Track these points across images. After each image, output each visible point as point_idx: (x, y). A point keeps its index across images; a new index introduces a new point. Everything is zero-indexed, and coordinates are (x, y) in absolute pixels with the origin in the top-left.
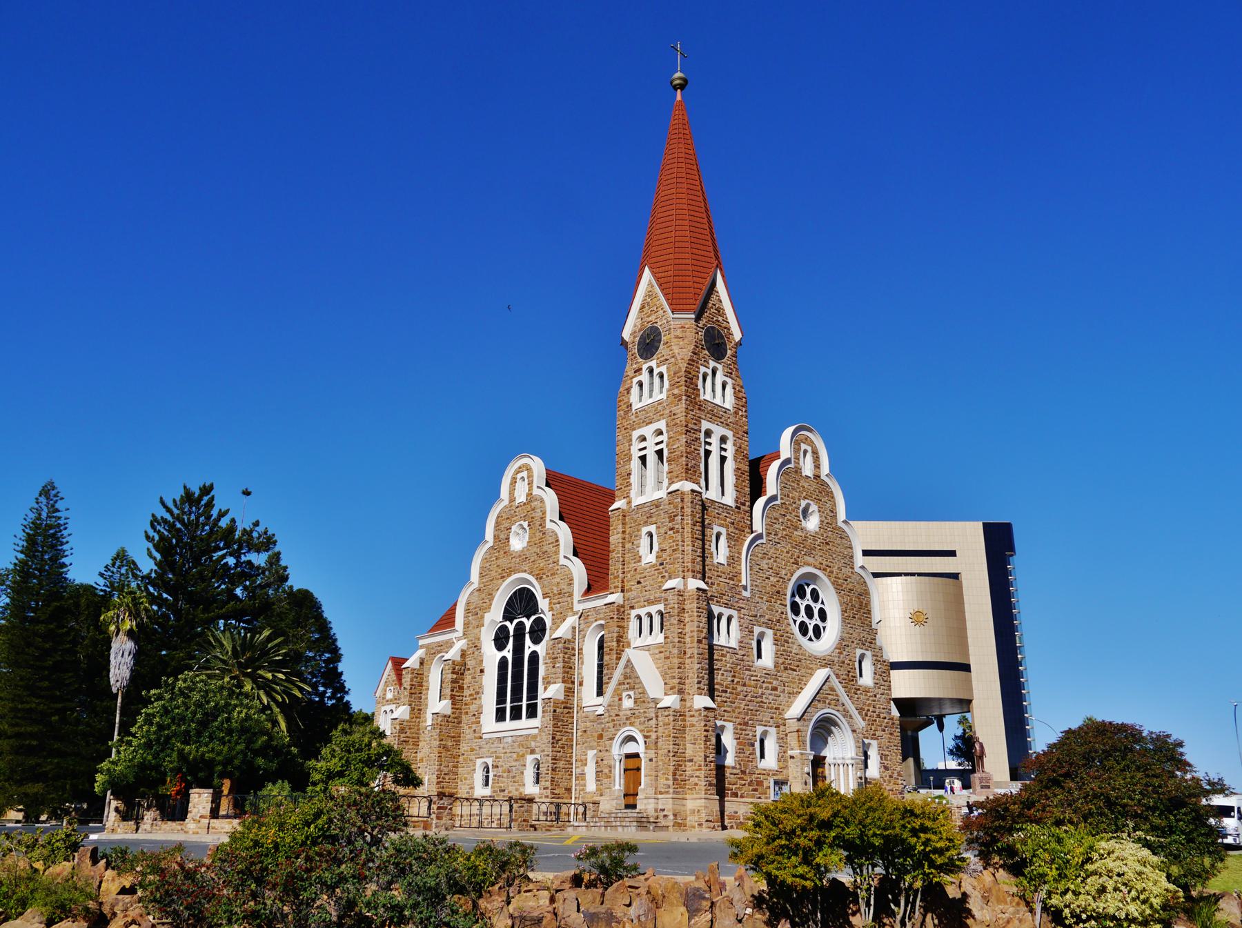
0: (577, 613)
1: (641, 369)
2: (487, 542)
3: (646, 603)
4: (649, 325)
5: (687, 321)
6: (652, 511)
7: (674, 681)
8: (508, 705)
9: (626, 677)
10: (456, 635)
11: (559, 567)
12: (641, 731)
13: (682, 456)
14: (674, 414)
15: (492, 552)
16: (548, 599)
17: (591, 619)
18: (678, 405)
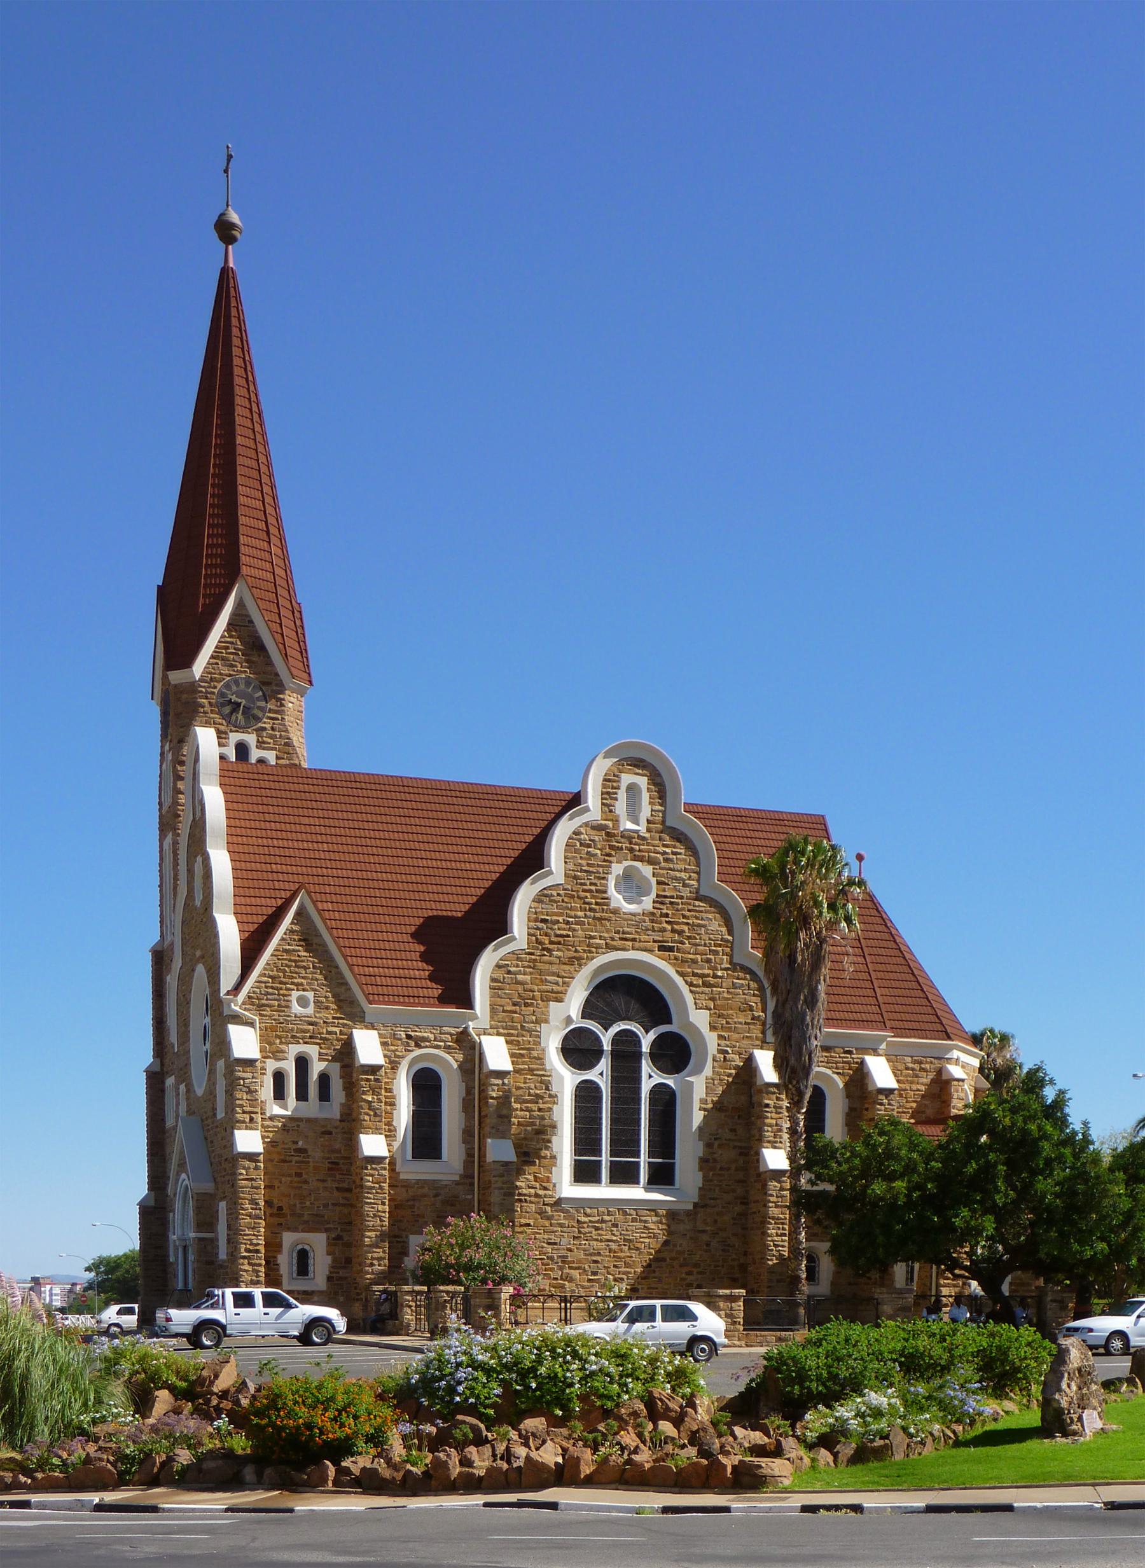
8: (605, 1158)
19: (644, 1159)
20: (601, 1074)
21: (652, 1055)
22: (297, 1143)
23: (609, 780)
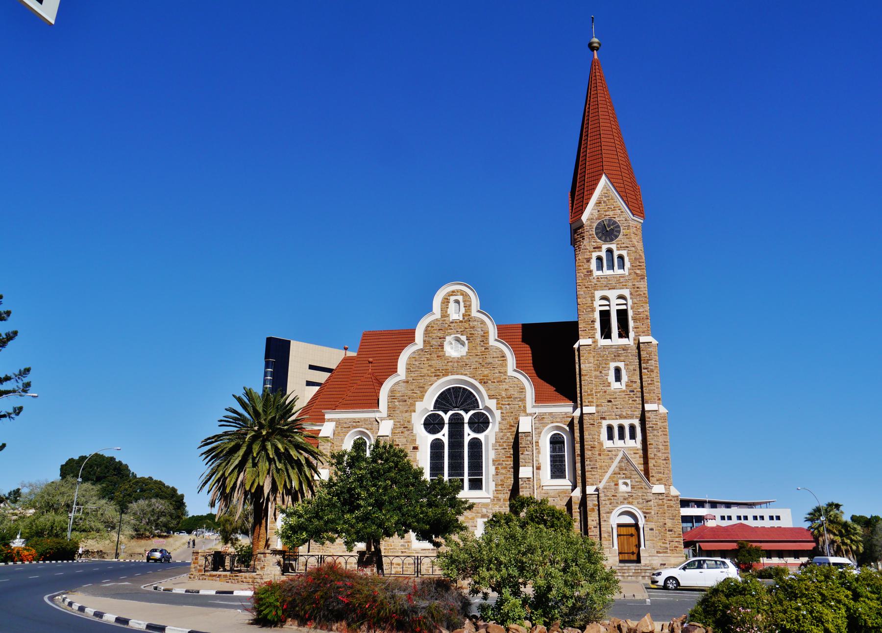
0: (531, 415)
1: (601, 247)
2: (416, 344)
3: (618, 417)
4: (607, 218)
5: (636, 223)
6: (620, 352)
7: (660, 475)
9: (621, 469)
10: (377, 415)
11: (507, 377)
12: (639, 509)
13: (648, 319)
14: (638, 288)
15: (422, 353)
16: (495, 400)
17: (546, 421)
18: (640, 281)
19: (466, 478)
21: (469, 423)
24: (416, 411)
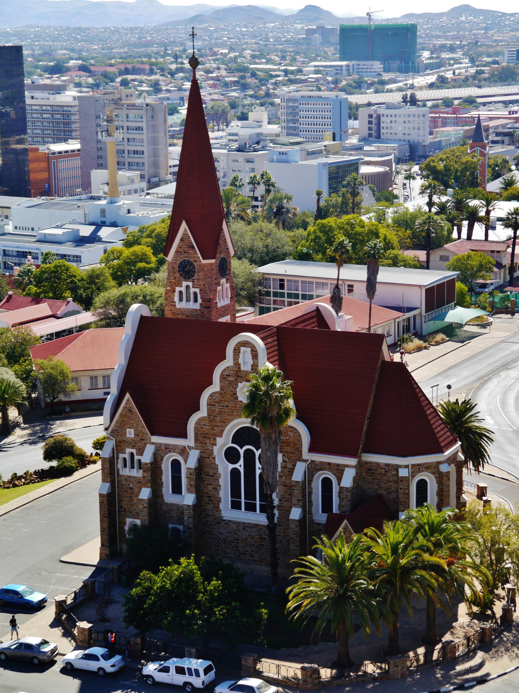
0: (305, 461)
20: (240, 466)
22: (129, 485)
23: (236, 349)
24: (217, 444)
